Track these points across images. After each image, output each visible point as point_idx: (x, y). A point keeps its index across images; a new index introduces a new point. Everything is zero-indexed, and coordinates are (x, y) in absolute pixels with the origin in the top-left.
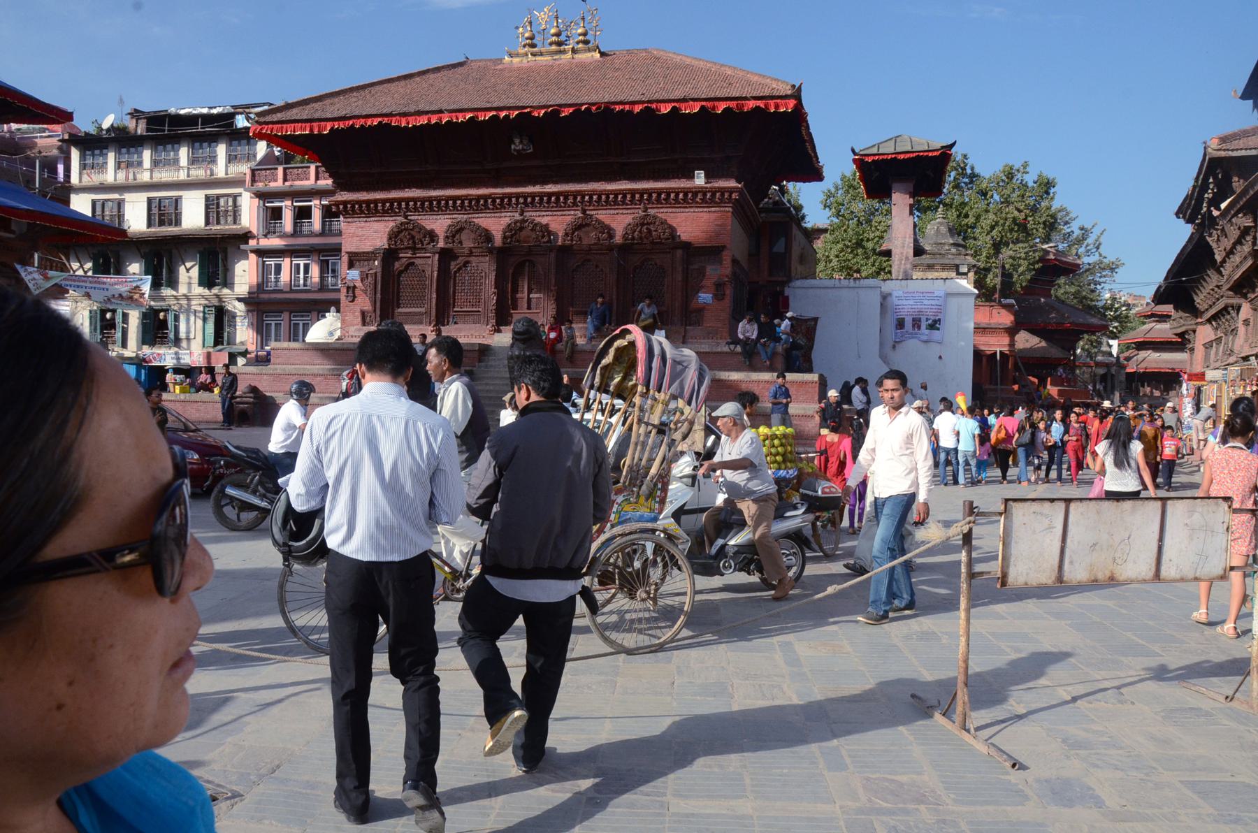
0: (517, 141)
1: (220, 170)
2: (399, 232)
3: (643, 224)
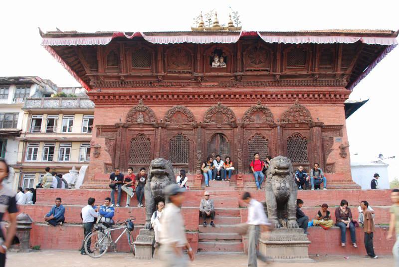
0: (217, 60)
2: (135, 113)
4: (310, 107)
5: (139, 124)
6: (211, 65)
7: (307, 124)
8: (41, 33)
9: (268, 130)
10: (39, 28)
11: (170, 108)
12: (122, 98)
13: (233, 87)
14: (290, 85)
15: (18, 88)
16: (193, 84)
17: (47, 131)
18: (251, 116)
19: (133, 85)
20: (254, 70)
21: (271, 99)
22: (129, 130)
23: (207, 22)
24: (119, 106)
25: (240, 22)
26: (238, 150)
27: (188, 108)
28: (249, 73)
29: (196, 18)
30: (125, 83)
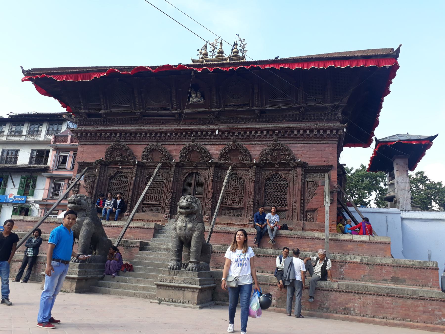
0: (193, 95)
1: (42, 137)
3: (274, 150)
4: (296, 145)
5: (117, 161)
6: (189, 100)
7: (289, 164)
8: (23, 71)
9: (244, 170)
10: (21, 67)
11: (147, 146)
12: (103, 136)
13: (212, 124)
14: (272, 120)
15: (51, 125)
16: (173, 121)
17: (58, 168)
18: (226, 155)
19: (114, 123)
20: (234, 105)
21: (251, 137)
22: (108, 168)
23: (211, 52)
24: (101, 143)
25: (246, 51)
26: (210, 190)
27: (164, 146)
28: (227, 109)
29: (200, 49)
30: (107, 121)
